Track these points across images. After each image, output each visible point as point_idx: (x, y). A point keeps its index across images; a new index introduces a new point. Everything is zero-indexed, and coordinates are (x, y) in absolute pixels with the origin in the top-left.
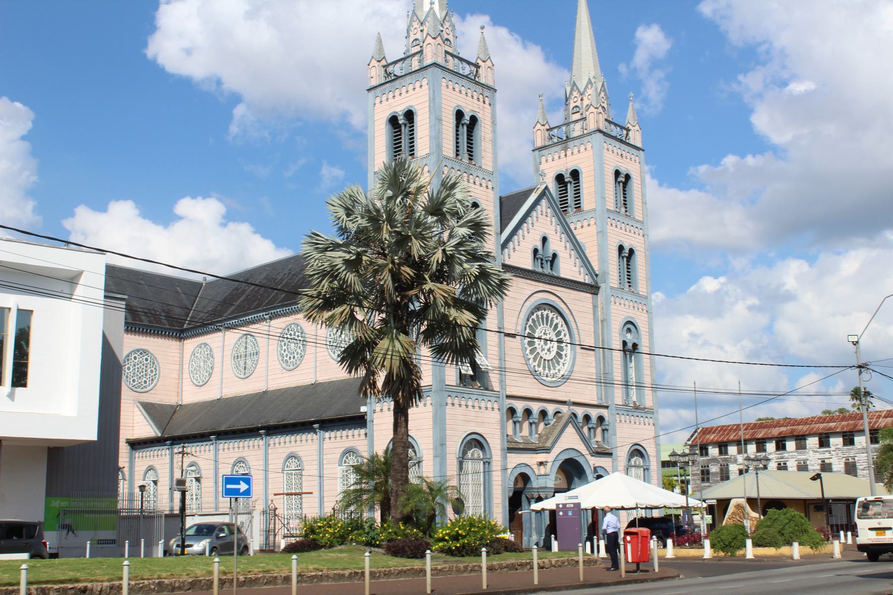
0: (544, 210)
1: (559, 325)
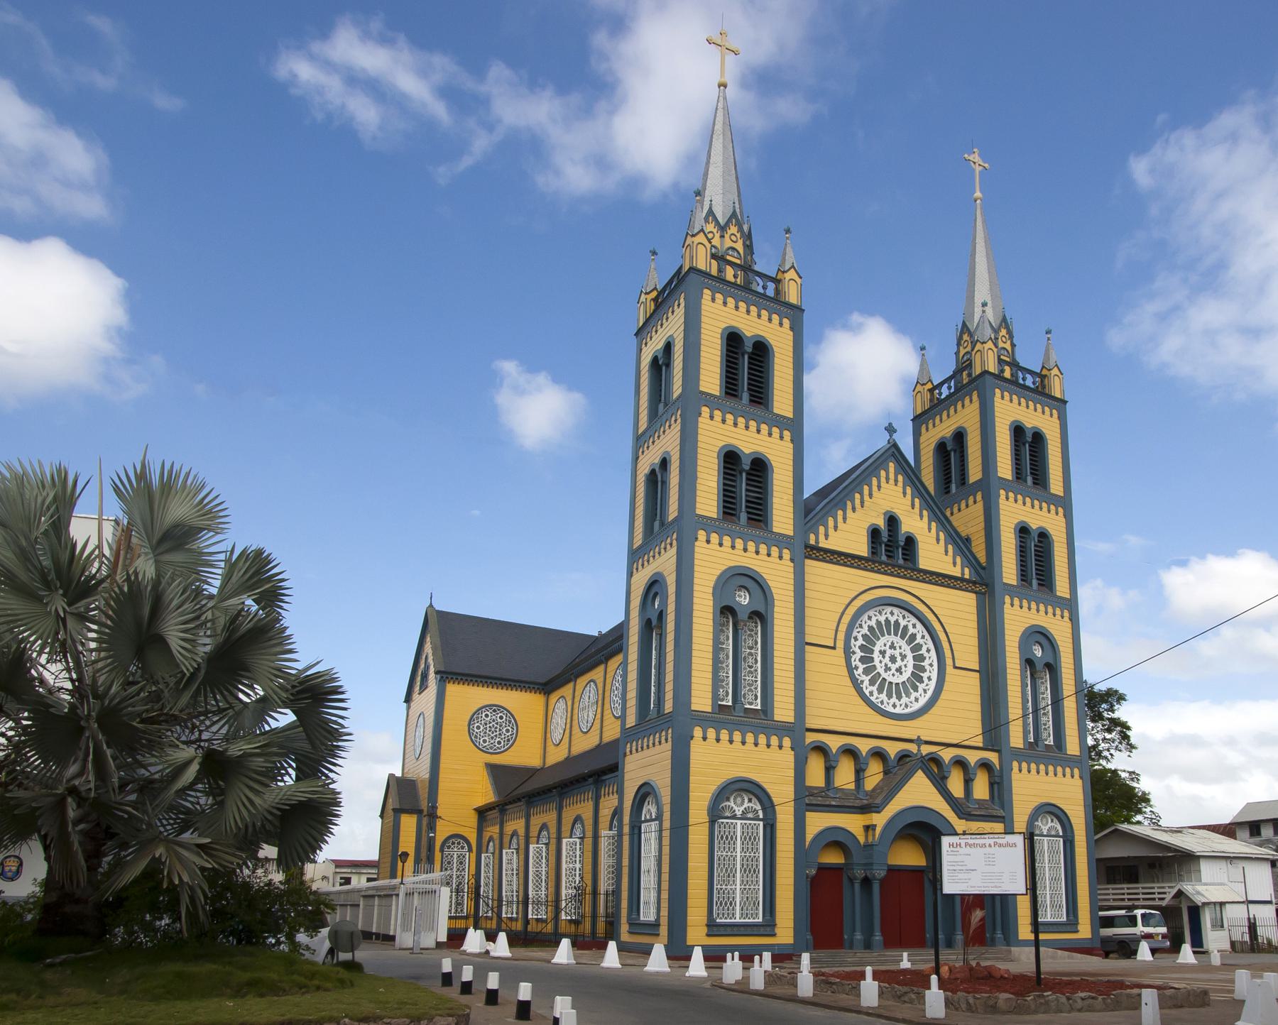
0: (892, 476)
1: (919, 637)
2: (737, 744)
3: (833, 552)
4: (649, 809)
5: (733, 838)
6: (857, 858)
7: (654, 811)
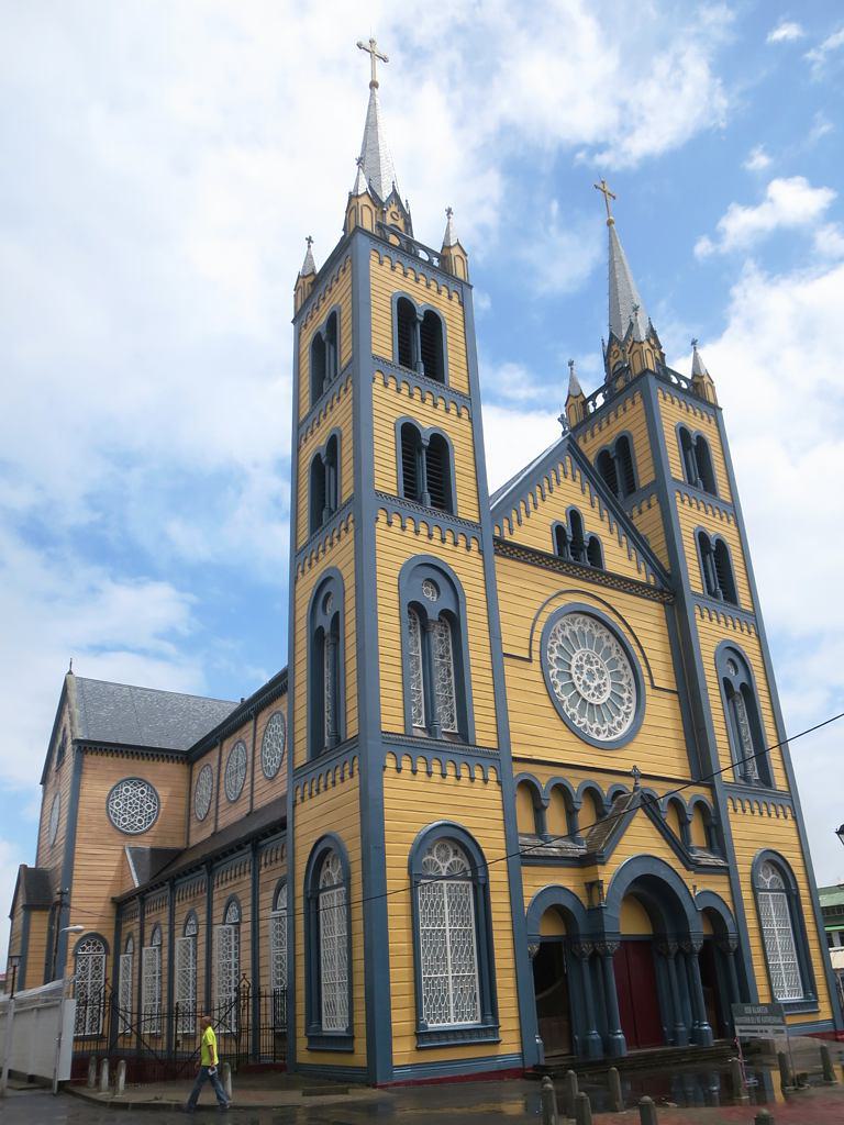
2: (436, 777)
3: (521, 548)
4: (333, 873)
5: (440, 906)
6: (583, 928)
7: (335, 876)
